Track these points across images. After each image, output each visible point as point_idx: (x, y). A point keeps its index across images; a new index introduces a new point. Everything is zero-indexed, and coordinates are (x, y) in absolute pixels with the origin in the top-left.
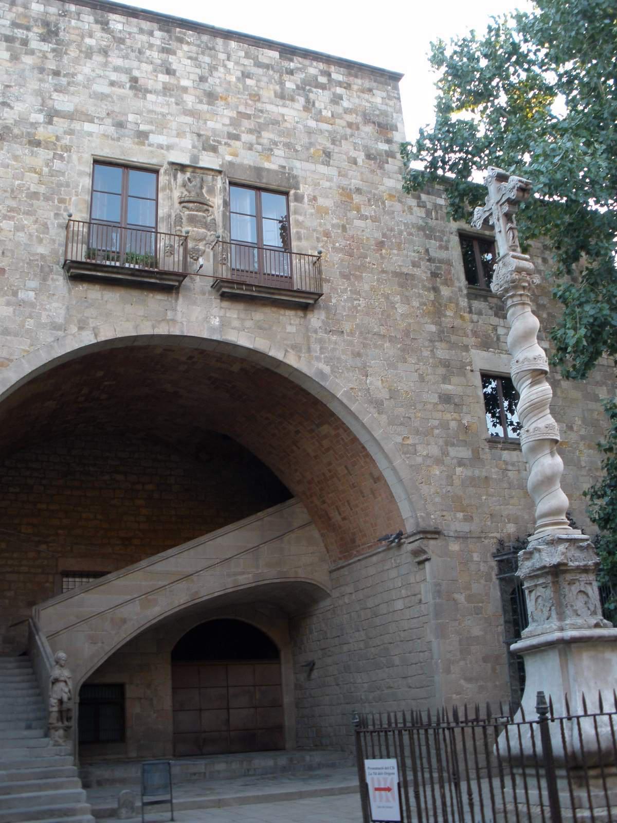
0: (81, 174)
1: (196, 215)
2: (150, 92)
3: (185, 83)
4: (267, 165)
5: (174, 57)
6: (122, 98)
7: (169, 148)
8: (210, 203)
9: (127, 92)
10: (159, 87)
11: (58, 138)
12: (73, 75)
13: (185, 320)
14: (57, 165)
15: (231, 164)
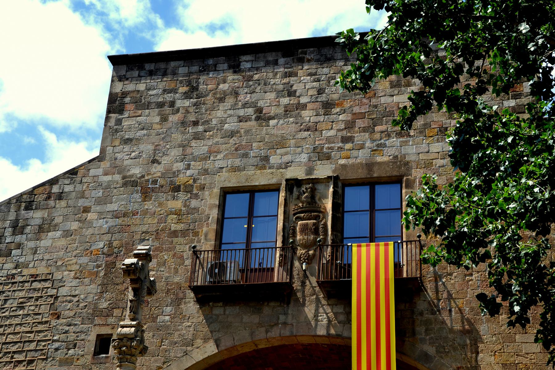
0: (211, 207)
1: (307, 224)
2: (273, 118)
3: (303, 100)
4: (379, 159)
5: (295, 78)
6: (247, 132)
7: (287, 165)
8: (322, 210)
9: (253, 123)
10: (281, 110)
11: (195, 181)
12: (207, 122)
13: (295, 321)
14: (194, 203)
15: (344, 166)
